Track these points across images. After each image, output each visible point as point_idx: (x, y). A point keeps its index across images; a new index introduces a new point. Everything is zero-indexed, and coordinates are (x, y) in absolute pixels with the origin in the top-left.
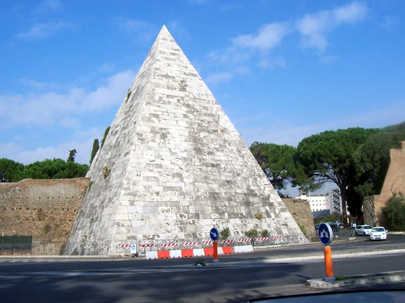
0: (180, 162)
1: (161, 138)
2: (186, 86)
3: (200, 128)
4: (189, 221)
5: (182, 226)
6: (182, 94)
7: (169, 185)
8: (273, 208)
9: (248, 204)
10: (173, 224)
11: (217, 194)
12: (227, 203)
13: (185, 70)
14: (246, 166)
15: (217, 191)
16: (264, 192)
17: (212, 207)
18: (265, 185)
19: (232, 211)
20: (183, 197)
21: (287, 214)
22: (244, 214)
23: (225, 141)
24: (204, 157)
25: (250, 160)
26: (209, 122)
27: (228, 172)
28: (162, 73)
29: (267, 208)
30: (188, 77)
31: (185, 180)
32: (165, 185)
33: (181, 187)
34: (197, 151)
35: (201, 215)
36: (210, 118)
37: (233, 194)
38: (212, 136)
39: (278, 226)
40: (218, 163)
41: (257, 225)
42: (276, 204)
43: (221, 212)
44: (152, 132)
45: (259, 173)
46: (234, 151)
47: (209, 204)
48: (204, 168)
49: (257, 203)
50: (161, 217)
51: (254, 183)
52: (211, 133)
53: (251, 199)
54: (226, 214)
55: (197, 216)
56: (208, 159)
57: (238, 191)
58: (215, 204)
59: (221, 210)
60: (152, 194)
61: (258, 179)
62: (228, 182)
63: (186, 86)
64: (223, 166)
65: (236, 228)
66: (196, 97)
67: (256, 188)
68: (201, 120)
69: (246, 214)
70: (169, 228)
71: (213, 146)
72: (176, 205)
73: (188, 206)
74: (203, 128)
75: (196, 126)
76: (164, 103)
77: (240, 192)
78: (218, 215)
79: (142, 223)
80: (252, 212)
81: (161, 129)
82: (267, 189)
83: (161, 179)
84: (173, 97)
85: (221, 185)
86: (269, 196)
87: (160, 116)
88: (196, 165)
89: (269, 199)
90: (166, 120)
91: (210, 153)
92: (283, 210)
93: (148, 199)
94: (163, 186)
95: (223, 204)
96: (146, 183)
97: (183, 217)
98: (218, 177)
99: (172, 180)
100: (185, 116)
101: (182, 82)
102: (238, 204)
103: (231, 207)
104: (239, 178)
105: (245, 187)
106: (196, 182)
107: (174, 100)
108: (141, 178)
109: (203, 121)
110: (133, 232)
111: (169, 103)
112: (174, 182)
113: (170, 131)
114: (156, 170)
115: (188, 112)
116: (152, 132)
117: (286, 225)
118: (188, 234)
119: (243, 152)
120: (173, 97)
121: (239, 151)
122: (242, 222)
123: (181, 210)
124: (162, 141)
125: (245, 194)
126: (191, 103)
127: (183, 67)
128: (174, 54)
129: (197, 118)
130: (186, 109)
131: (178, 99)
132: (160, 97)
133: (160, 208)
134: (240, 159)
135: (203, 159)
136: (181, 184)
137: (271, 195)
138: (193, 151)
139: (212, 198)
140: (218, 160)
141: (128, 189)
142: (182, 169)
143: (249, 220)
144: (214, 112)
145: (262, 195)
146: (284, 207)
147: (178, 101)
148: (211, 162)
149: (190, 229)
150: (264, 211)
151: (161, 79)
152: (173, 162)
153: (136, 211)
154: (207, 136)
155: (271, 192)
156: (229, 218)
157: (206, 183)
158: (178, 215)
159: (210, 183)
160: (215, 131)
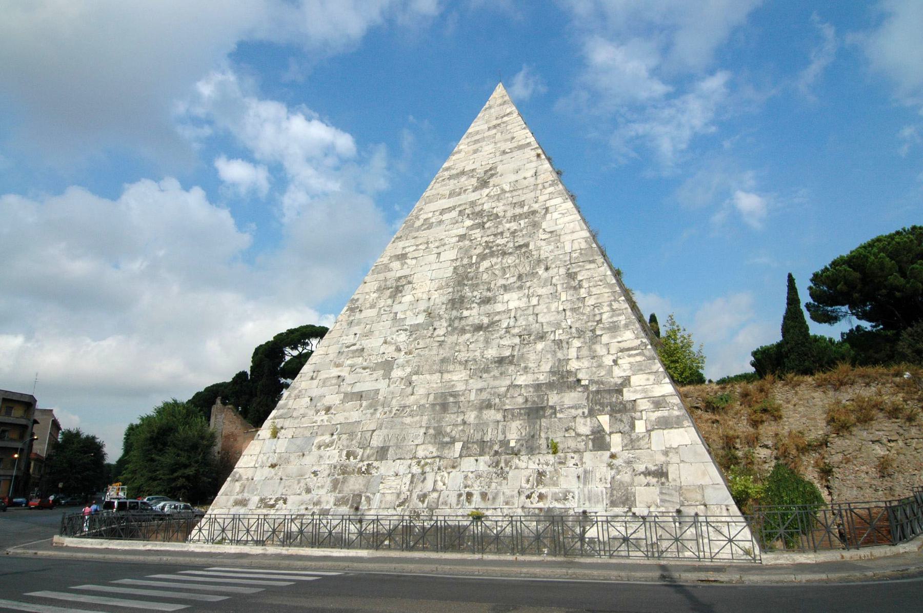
0: (402, 337)
1: (390, 297)
2: (492, 175)
3: (487, 251)
4: (360, 465)
5: (341, 477)
8: (625, 418)
10: (327, 472)
11: (455, 395)
12: (471, 417)
14: (573, 310)
15: (460, 387)
16: (610, 372)
17: (428, 428)
18: (622, 351)
19: (478, 436)
20: (372, 411)
21: (686, 436)
22: (512, 444)
23: (539, 261)
24: (466, 313)
25: (594, 291)
27: (514, 335)
28: (454, 172)
29: (604, 420)
31: (397, 373)
32: (349, 389)
33: (377, 392)
34: (453, 304)
35: (391, 452)
36: (522, 222)
37: (503, 389)
38: (510, 260)
39: (625, 477)
40: (497, 318)
41: (541, 474)
42: (644, 405)
43: (447, 439)
45: (615, 319)
46: (554, 281)
47: (424, 424)
49: (569, 408)
51: (585, 352)
52: (510, 254)
53: (553, 398)
54: (458, 446)
56: (474, 314)
57: (521, 380)
58: (439, 421)
59: (448, 434)
60: (317, 412)
61: (605, 339)
62: (501, 361)
65: (469, 483)
66: (507, 188)
67: (585, 363)
68: (495, 235)
69: (518, 441)
70: (312, 482)
71: (501, 282)
72: (350, 430)
73: (374, 431)
74: (494, 249)
76: (430, 226)
77: (523, 384)
78: (434, 450)
80: (543, 435)
81: (400, 278)
82: (625, 362)
83: (349, 379)
86: (626, 381)
87: (409, 255)
88: (435, 334)
89: (620, 392)
90: (416, 258)
91: (486, 301)
92: (665, 424)
93: (306, 423)
94: (346, 394)
95: (459, 420)
96: (315, 393)
97: (352, 458)
98: (478, 354)
99: (368, 378)
101: (486, 172)
102: (504, 417)
103: (481, 426)
104: (540, 346)
105: (546, 367)
106: (416, 373)
108: (315, 382)
109: (502, 233)
110: (248, 492)
111: (440, 222)
114: (349, 362)
115: (471, 228)
117: (661, 474)
118: (343, 498)
119: (579, 278)
121: (571, 276)
122: (497, 463)
123: (354, 442)
124: (389, 301)
125: (538, 387)
127: (506, 141)
128: (495, 127)
129: (489, 232)
131: (464, 207)
132: (425, 220)
133: (317, 440)
135: (461, 319)
136: (382, 385)
137: (635, 380)
138: (444, 306)
139: (438, 408)
140: (499, 313)
141: (286, 405)
142: (400, 350)
144: (536, 207)
145: (597, 382)
146: (676, 413)
148: (477, 322)
149: (355, 484)
151: (445, 185)
152: (389, 339)
153: (274, 448)
154: (496, 264)
155: (638, 369)
156: (461, 456)
157: (440, 372)
158: (344, 453)
159: (449, 372)
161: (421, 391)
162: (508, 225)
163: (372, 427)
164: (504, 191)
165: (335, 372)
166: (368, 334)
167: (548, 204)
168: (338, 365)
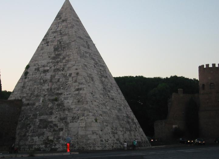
15: (118, 115)
20: (109, 117)
64: (115, 99)
75: (100, 73)
85: (118, 111)
91: (109, 91)
109: (101, 70)
130: (94, 62)
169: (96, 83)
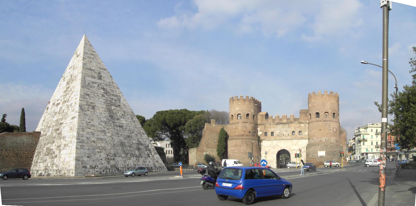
6: (99, 81)
7: (99, 137)
9: (139, 149)
11: (123, 143)
12: (128, 148)
13: (99, 65)
15: (123, 141)
26: (115, 100)
30: (102, 70)
31: (108, 134)
38: (118, 109)
44: (87, 105)
48: (116, 128)
50: (97, 156)
53: (140, 147)
55: (115, 155)
62: (128, 136)
63: (101, 76)
64: (125, 127)
72: (104, 148)
75: (109, 102)
76: (91, 87)
79: (89, 159)
81: (91, 103)
84: (95, 83)
86: (148, 146)
91: (118, 119)
96: (88, 136)
100: (103, 96)
101: (99, 73)
103: (131, 151)
104: (133, 134)
107: (96, 85)
108: (85, 133)
109: (112, 99)
112: (101, 136)
113: (96, 104)
114: (92, 128)
116: (87, 105)
119: (134, 119)
120: (95, 83)
124: (93, 111)
126: (105, 87)
133: (96, 150)
134: (133, 123)
136: (106, 137)
143: (140, 159)
144: (117, 94)
147: (98, 85)
149: (112, 162)
150: (146, 153)
160: (119, 106)
161: (116, 141)
162: (113, 97)
163: (110, 148)
164: (107, 84)
165: (90, 131)
166: (92, 120)
167: (120, 95)
168: (89, 128)
169: (97, 111)
